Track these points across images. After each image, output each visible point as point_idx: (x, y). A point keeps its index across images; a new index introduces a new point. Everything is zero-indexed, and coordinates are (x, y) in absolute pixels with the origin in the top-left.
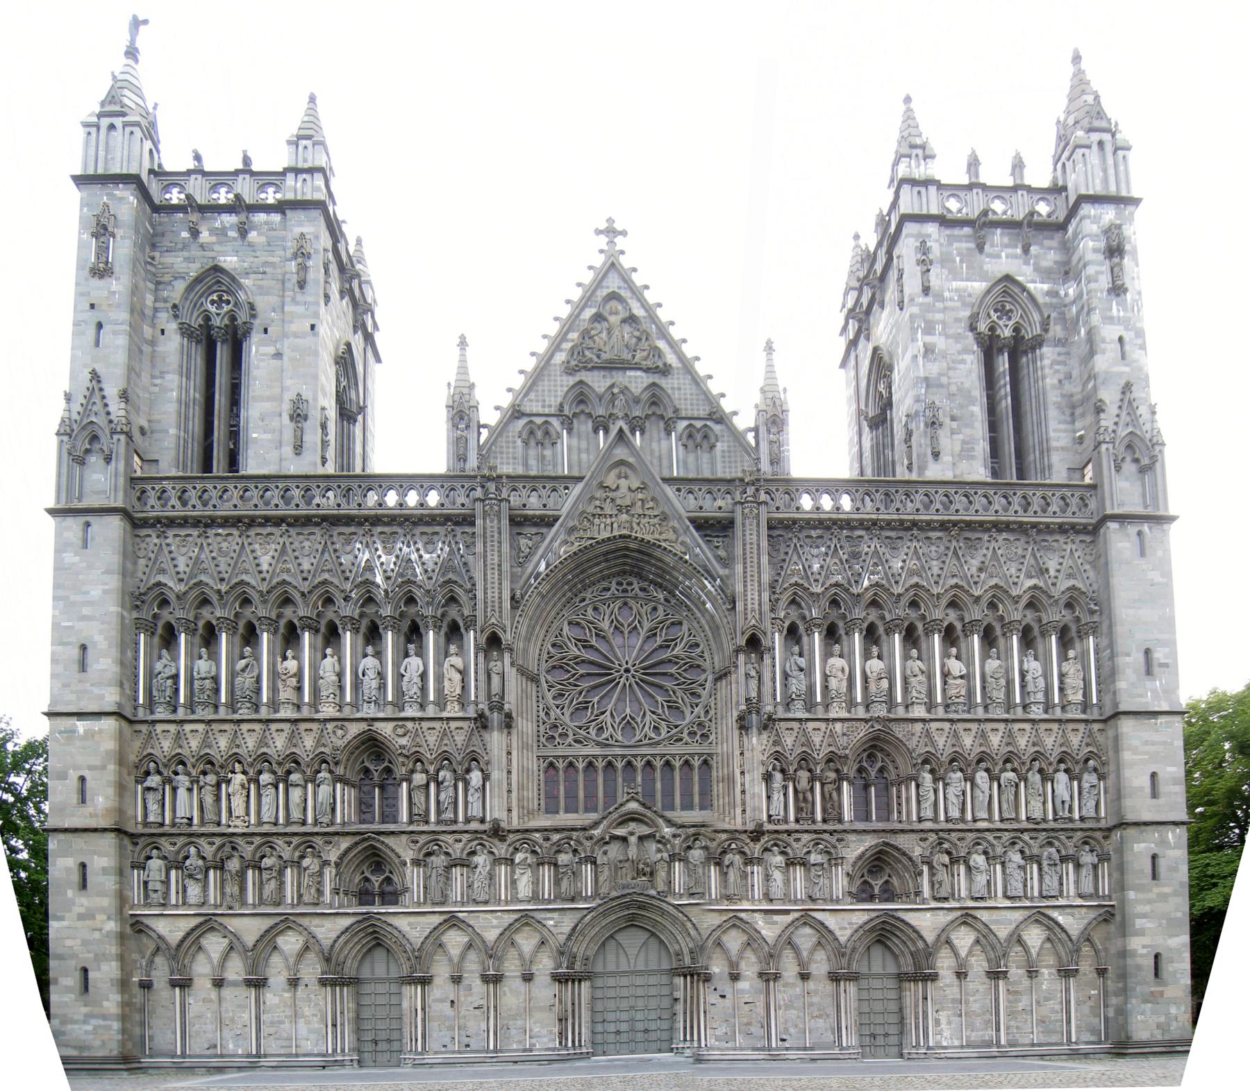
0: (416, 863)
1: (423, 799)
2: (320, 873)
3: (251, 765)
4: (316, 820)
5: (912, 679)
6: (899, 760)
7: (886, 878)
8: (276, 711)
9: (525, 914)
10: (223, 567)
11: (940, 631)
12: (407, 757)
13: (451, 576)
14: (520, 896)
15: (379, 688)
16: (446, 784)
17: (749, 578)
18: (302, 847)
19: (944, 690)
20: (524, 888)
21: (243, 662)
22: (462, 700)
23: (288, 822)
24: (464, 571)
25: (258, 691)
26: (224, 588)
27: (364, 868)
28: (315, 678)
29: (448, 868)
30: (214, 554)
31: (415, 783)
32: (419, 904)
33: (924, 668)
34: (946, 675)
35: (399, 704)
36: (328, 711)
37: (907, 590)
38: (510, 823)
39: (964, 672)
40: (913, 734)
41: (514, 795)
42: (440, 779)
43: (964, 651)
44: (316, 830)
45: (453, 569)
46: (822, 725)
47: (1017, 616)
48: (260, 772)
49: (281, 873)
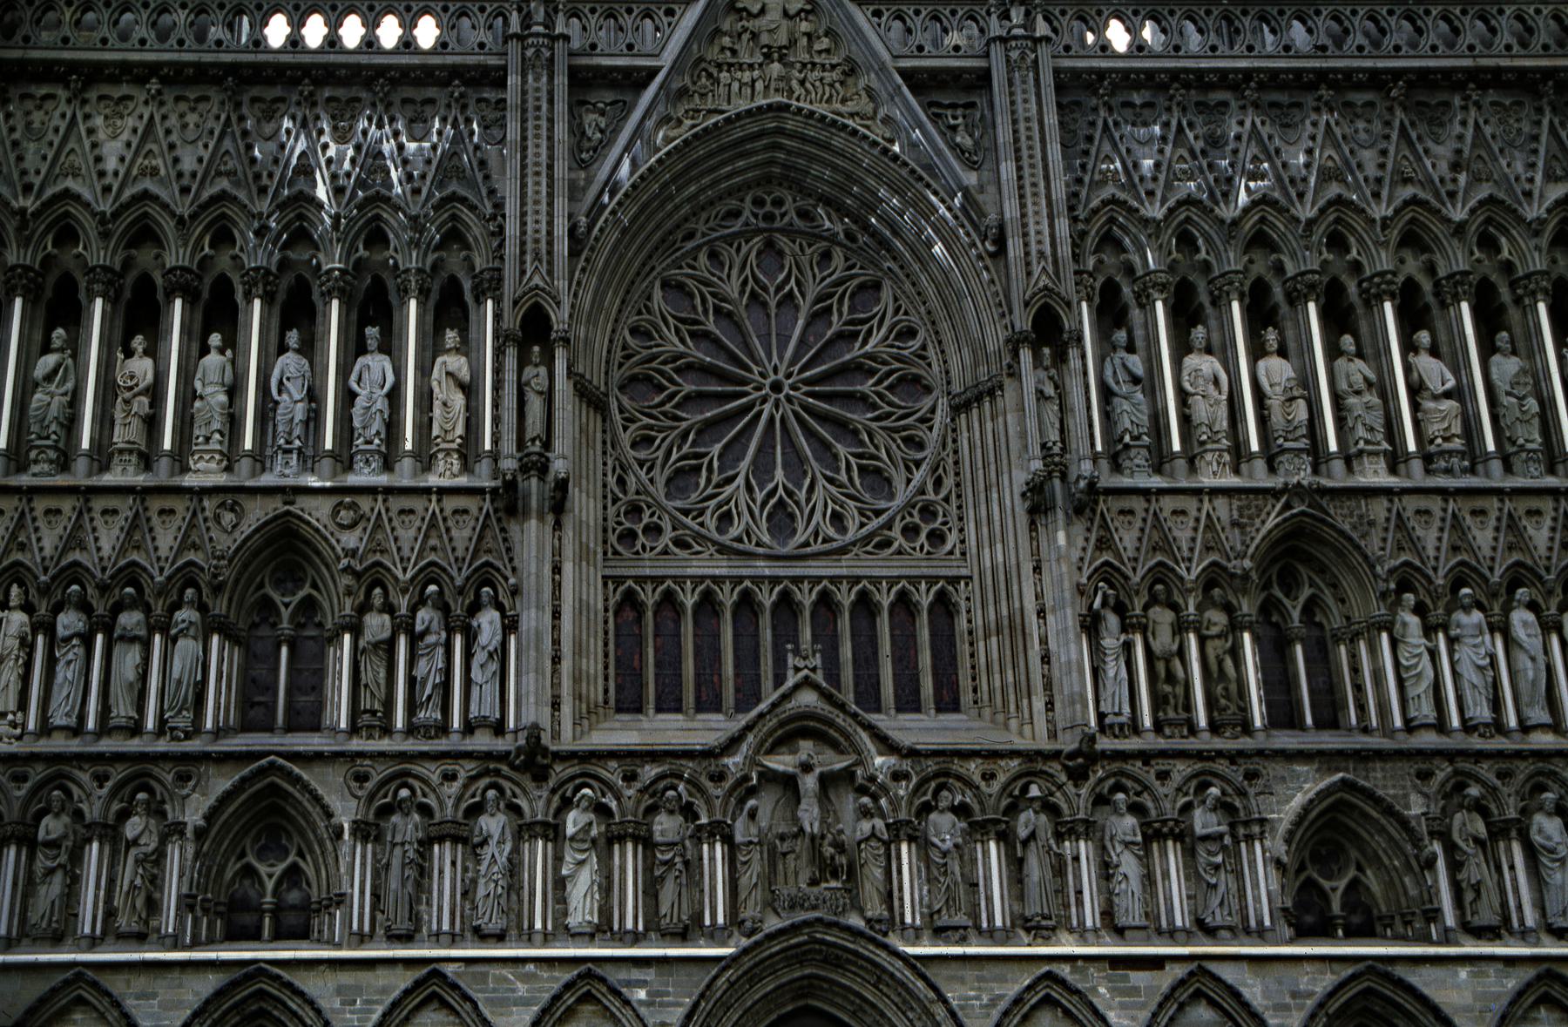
0: (363, 831)
1: (382, 674)
2: (159, 857)
3: (45, 591)
4: (161, 721)
5: (1352, 400)
6: (1347, 583)
7: (1352, 873)
8: (105, 468)
9: (589, 971)
10: (31, 162)
11: (1392, 297)
12: (358, 575)
13: (454, 187)
14: (574, 920)
15: (306, 423)
16: (431, 639)
17: (1028, 190)
18: (128, 790)
19: (1417, 424)
20: (582, 909)
21: (50, 360)
22: (468, 453)
23: (104, 729)
24: (479, 176)
25: (71, 423)
26: (29, 203)
27: (248, 842)
28: (188, 396)
29: (426, 844)
30: (17, 135)
31: (368, 637)
32: (362, 939)
33: (1372, 376)
34: (1415, 390)
35: (344, 458)
36: (205, 472)
37: (1322, 211)
38: (556, 735)
39: (1451, 383)
40: (1372, 524)
41: (566, 666)
42: (419, 627)
43: (1443, 337)
44: (162, 746)
45: (460, 174)
46: (1190, 504)
47: (1538, 263)
48: (57, 609)
49: (77, 857)
